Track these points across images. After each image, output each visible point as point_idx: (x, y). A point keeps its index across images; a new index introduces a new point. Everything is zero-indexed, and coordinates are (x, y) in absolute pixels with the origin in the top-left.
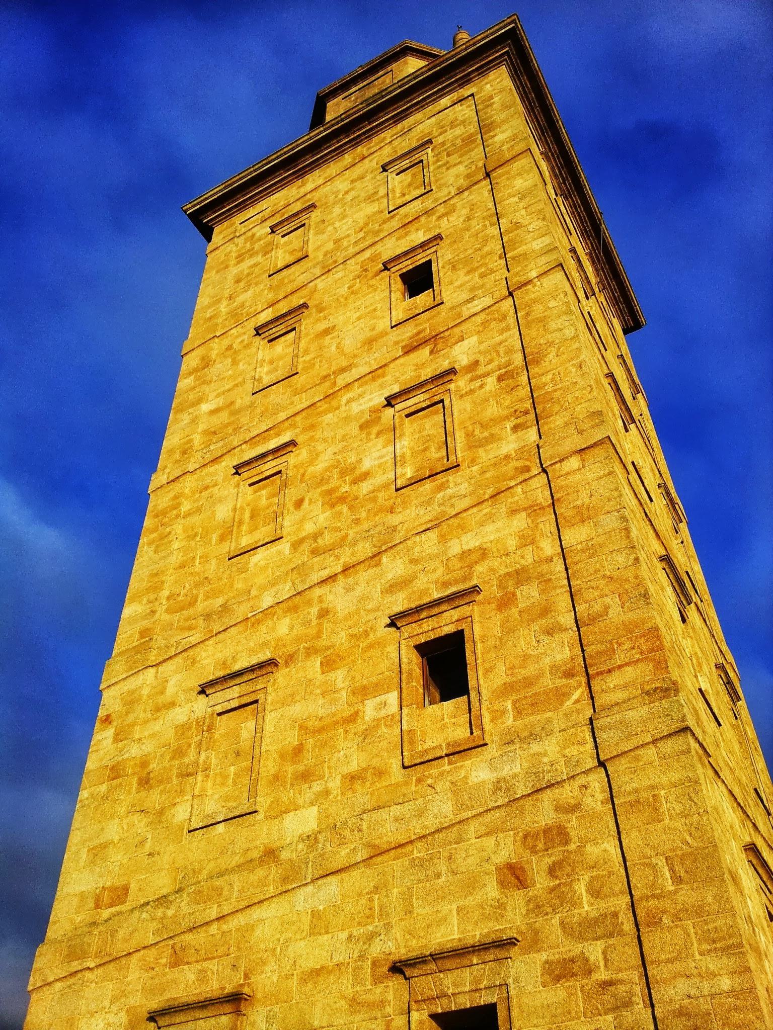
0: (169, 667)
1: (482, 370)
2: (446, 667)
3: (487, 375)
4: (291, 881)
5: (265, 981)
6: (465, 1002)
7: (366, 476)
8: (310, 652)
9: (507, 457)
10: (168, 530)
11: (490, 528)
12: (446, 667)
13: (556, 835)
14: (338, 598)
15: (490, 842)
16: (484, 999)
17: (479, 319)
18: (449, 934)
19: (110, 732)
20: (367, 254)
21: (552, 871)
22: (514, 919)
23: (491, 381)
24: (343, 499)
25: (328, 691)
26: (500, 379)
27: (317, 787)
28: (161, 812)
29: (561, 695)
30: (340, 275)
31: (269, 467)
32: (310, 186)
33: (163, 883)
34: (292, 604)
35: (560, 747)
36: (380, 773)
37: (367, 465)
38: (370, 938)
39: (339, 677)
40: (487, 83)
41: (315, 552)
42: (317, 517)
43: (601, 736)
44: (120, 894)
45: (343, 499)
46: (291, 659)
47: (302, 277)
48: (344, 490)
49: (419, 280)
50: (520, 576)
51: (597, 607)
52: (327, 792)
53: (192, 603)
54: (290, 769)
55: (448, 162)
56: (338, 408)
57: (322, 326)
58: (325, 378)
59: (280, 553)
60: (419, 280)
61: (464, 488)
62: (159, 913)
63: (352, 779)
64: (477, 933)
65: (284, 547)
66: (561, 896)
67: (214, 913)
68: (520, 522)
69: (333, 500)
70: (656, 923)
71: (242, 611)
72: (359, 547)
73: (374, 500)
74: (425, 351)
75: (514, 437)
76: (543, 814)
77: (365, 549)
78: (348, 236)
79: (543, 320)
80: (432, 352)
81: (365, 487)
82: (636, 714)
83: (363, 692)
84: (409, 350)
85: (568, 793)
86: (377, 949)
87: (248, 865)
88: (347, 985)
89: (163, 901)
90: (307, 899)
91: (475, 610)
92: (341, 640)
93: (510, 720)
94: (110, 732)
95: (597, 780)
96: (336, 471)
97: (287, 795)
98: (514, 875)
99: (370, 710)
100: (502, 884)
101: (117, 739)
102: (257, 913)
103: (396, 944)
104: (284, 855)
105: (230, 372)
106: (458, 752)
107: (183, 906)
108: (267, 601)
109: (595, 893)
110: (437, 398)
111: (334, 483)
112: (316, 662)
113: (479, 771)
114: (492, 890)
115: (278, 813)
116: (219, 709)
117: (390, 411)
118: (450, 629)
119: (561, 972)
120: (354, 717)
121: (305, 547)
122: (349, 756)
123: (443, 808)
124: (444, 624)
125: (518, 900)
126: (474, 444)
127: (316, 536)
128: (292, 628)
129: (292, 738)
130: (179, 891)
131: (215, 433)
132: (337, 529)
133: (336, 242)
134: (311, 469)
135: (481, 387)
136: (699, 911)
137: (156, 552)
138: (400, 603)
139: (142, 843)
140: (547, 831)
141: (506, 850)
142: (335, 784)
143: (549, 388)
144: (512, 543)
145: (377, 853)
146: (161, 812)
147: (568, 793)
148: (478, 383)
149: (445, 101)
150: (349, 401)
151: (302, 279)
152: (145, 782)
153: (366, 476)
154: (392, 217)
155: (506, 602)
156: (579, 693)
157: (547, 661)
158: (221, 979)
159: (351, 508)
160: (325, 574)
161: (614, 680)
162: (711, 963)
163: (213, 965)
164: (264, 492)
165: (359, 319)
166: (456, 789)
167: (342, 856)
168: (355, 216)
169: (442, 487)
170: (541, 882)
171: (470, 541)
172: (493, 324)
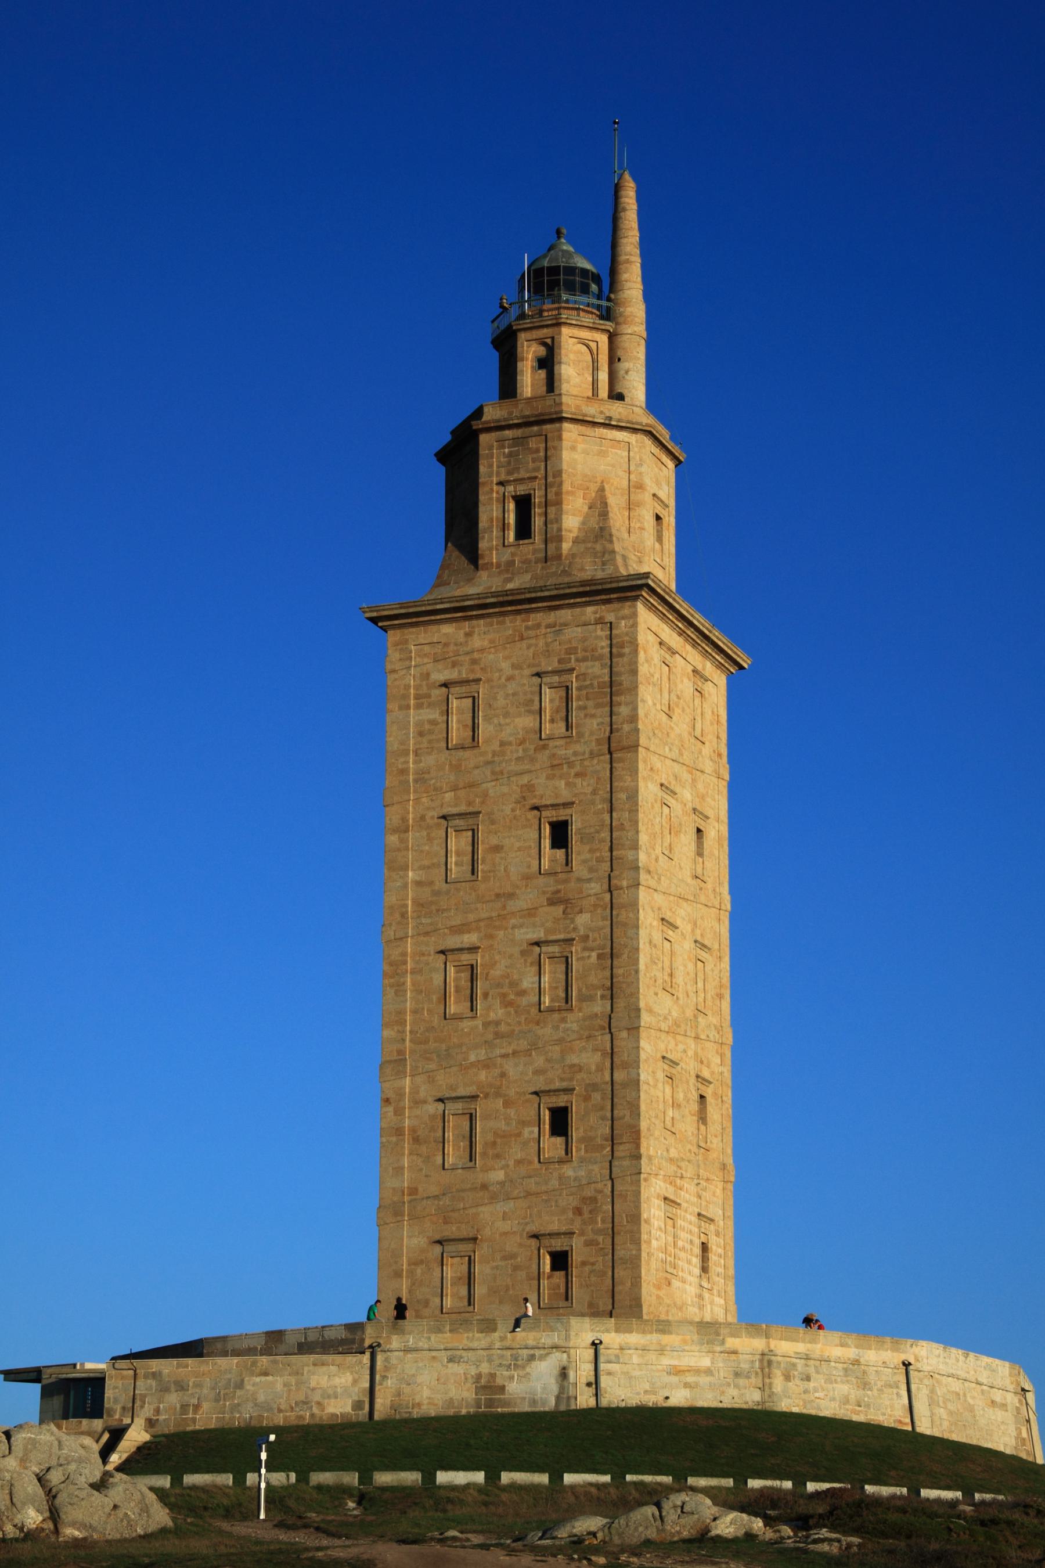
0: (419, 1079)
1: (590, 944)
2: (560, 1121)
3: (592, 950)
4: (494, 1198)
6: (559, 1249)
8: (498, 1095)
9: (596, 1015)
10: (402, 980)
11: (584, 1055)
12: (560, 1121)
13: (593, 1200)
14: (512, 1069)
15: (571, 1198)
17: (592, 899)
18: (554, 1227)
21: (590, 1212)
22: (576, 1227)
23: (594, 954)
24: (511, 1004)
25: (508, 1119)
26: (600, 957)
27: (503, 1162)
28: (428, 1157)
29: (603, 1147)
30: (505, 789)
31: (466, 958)
32: (477, 642)
33: (434, 1190)
34: (487, 1064)
35: (599, 1170)
36: (530, 1163)
38: (527, 1224)
39: (512, 1112)
40: (623, 618)
41: (498, 1035)
42: (498, 1012)
43: (614, 1169)
44: (413, 1191)
45: (511, 1004)
46: (487, 1096)
47: (476, 772)
48: (512, 997)
49: (560, 835)
50: (594, 1087)
51: (621, 1114)
52: (508, 1166)
53: (426, 1042)
54: (491, 1152)
55: (585, 708)
56: (506, 929)
57: (494, 841)
58: (498, 895)
59: (477, 1027)
61: (575, 1026)
62: (436, 1202)
63: (519, 1162)
64: (564, 1229)
65: (479, 1022)
68: (597, 1057)
69: (507, 1004)
70: (619, 1234)
72: (521, 1041)
73: (528, 1012)
74: (561, 908)
75: (599, 1002)
76: (589, 1192)
77: (523, 1044)
78: (510, 743)
79: (625, 925)
80: (564, 912)
81: (524, 1001)
82: (626, 1163)
83: (524, 1123)
84: (551, 902)
85: (600, 1186)
86: (528, 1228)
87: (473, 1189)
88: (518, 1239)
89: (436, 1197)
90: (501, 1207)
92: (512, 1093)
93: (583, 1152)
95: (609, 1183)
96: (507, 981)
98: (578, 1211)
100: (574, 1213)
101: (396, 1113)
102: (481, 1209)
103: (533, 1228)
104: (491, 1188)
105: (427, 848)
106: (561, 1162)
107: (446, 1201)
108: (472, 1058)
109: (603, 1221)
110: (565, 954)
111: (505, 990)
112: (501, 1101)
113: (568, 1171)
114: (570, 1215)
115: (486, 1170)
116: (452, 1112)
117: (537, 949)
118: (562, 1104)
119: (588, 1243)
120: (519, 1135)
121: (491, 1029)
122: (516, 1152)
124: (561, 1101)
125: (578, 1220)
126: (582, 999)
127: (497, 1023)
128: (487, 1077)
129: (490, 1137)
130: (444, 1194)
131: (422, 905)
132: (509, 1024)
133: (502, 744)
134: (492, 972)
135: (589, 957)
136: (632, 1232)
137: (396, 993)
138: (540, 1084)
139: (421, 1170)
140: (590, 1198)
141: (575, 1203)
142: (511, 1163)
143: (621, 979)
144: (593, 1068)
145: (528, 1194)
146: (428, 1157)
148: (586, 954)
150: (513, 928)
152: (416, 1140)
153: (522, 993)
154: (544, 747)
155: (587, 1098)
156: (609, 1149)
157: (599, 1132)
158: (465, 1232)
159: (516, 1012)
160: (503, 1051)
161: (621, 1148)
162: (632, 1247)
163: (463, 1226)
164: (463, 975)
165: (519, 849)
168: (517, 720)
169: (563, 1020)
170: (586, 1215)
171: (573, 1059)
172: (599, 911)
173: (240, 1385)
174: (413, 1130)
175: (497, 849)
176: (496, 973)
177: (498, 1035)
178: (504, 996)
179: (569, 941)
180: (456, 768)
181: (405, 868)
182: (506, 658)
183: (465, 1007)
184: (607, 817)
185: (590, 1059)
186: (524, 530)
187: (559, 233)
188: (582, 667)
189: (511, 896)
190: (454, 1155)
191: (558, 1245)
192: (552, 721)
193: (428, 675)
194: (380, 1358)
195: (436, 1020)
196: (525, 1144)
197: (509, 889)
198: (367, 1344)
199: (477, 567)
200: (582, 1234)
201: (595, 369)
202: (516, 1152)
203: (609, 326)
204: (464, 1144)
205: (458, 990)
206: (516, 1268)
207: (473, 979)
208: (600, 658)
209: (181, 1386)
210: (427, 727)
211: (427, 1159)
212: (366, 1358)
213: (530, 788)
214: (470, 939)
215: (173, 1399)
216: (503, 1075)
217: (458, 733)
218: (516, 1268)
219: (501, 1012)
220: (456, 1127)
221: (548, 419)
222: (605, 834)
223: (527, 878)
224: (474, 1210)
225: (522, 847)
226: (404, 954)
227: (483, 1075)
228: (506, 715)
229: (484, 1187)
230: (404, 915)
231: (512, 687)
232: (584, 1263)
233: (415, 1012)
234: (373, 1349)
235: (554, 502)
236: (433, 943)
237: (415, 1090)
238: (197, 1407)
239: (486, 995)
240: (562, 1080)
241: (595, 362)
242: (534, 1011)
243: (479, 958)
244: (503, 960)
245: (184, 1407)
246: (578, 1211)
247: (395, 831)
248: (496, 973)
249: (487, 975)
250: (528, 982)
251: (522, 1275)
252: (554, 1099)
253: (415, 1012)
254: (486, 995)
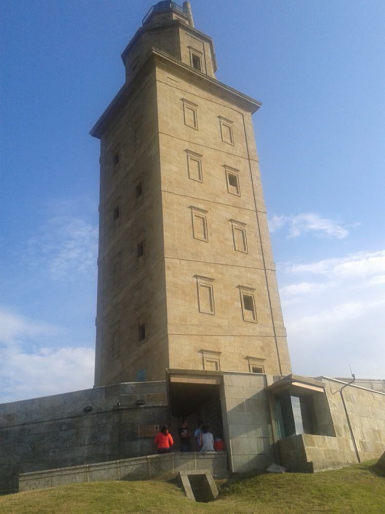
6: (257, 367)
16: (261, 367)
26: (255, 235)
49: (233, 180)
56: (217, 209)
67: (210, 334)
74: (237, 210)
86: (243, 352)
103: (245, 353)
104: (224, 328)
114: (260, 350)
147: (270, 338)
149: (235, 107)
153: (227, 239)
167: (235, 333)
183: (202, 236)
189: (218, 196)
190: (205, 307)
191: (258, 364)
220: (204, 292)
224: (216, 337)
227: (212, 270)
229: (220, 326)
239: (211, 234)
243: (208, 216)
246: (263, 349)
249: (211, 225)
250: (229, 235)
252: (245, 291)
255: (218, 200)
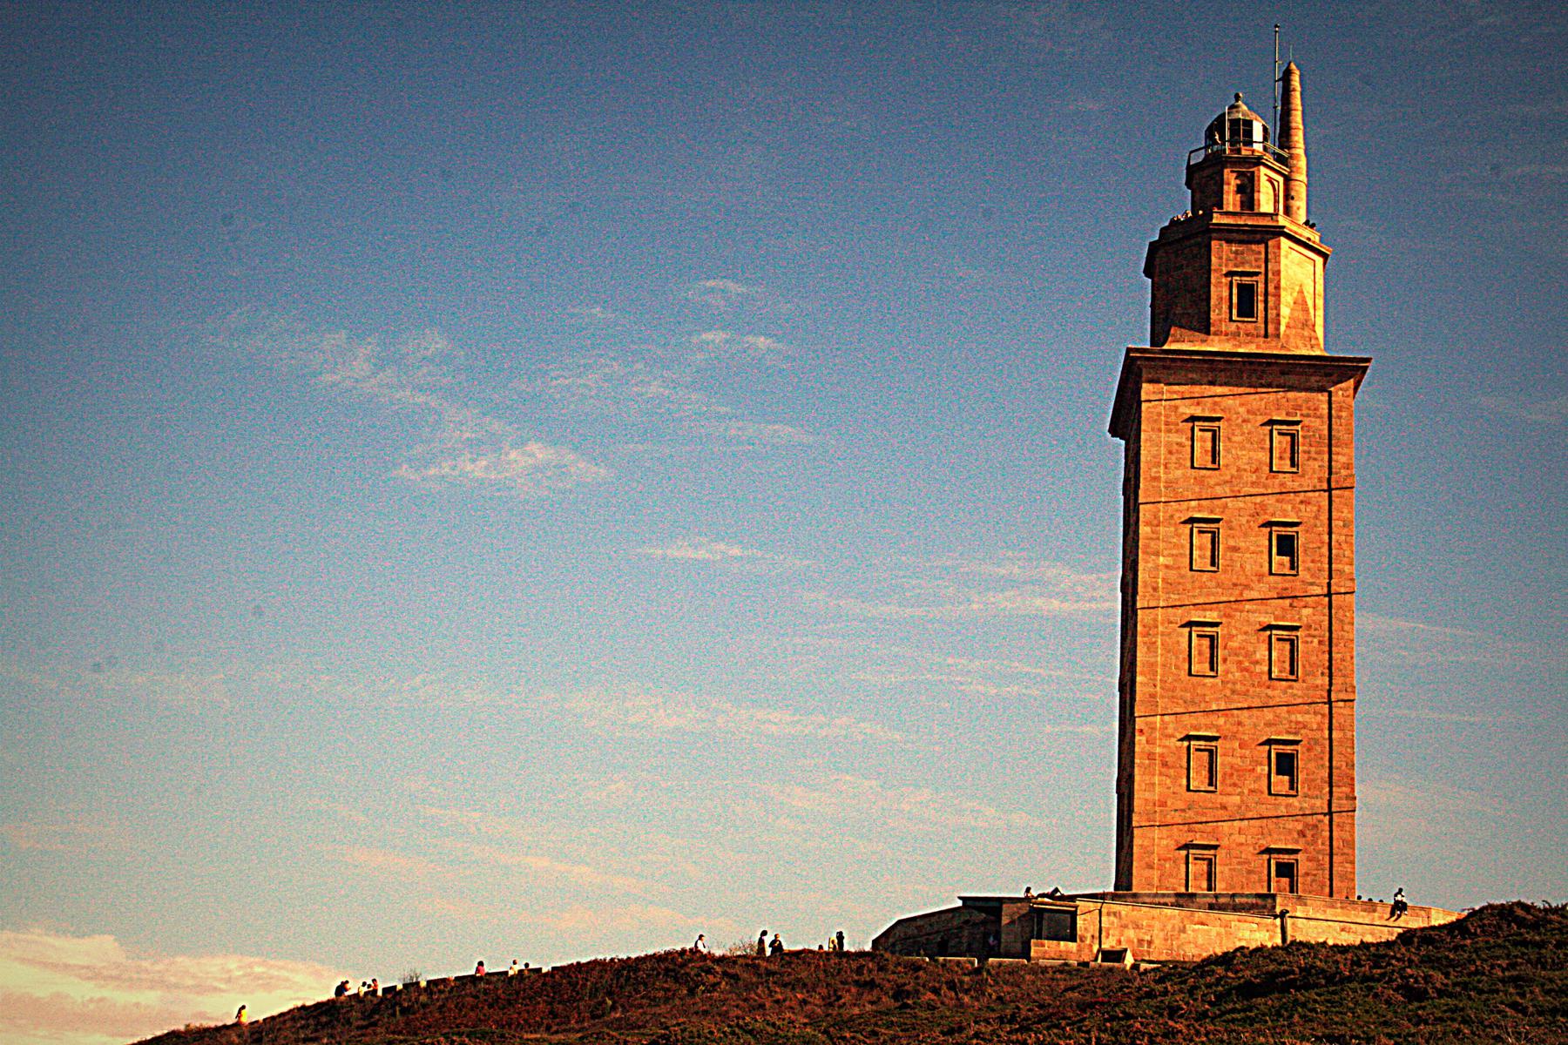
0: (1167, 718)
5: (1224, 842)
7: (1257, 662)
8: (1234, 737)
12: (1286, 765)
19: (1143, 738)
20: (1258, 499)
24: (1246, 670)
26: (1320, 642)
30: (1241, 505)
33: (1181, 805)
37: (1258, 656)
45: (1246, 670)
49: (1287, 546)
50: (1317, 742)
57: (1232, 543)
60: (1287, 546)
63: (1251, 791)
65: (1217, 680)
66: (1314, 842)
71: (1203, 706)
91: (1299, 748)
94: (1143, 738)
97: (1230, 789)
98: (1302, 834)
99: (1259, 769)
103: (1264, 843)
119: (1309, 860)
122: (1250, 784)
123: (1282, 811)
125: (1302, 840)
141: (1300, 827)
151: (1219, 491)
152: (1165, 764)
153: (1257, 662)
166: (1287, 806)
167: (1250, 815)
169: (1291, 687)
173: (1183, 930)
174: (1162, 755)
175: (1235, 549)
176: (1234, 644)
177: (1233, 692)
178: (1240, 662)
179: (1296, 628)
180: (1200, 482)
181: (1157, 554)
182: (1242, 405)
184: (1326, 538)
185: (1313, 719)
186: (1246, 309)
187: (1237, 98)
188: (1306, 421)
189: (1247, 587)
190: (1199, 780)
191: (1285, 858)
192: (1281, 458)
193: (1176, 407)
194: (1289, 922)
195: (1183, 674)
196: (1259, 777)
197: (1243, 580)
198: (1278, 910)
199: (1208, 333)
200: (1306, 851)
201: (1276, 202)
202: (1250, 784)
203: (1286, 171)
204: (1205, 773)
205: (1200, 653)
206: (1249, 872)
207: (1213, 647)
208: (1320, 417)
209: (1137, 927)
210: (1175, 447)
211: (1175, 779)
212: (1278, 921)
213: (1263, 507)
214: (1211, 616)
215: (1131, 933)
216: (1239, 723)
217: (1203, 457)
218: (1249, 872)
219: (1238, 675)
220: (1199, 760)
221: (1268, 234)
222: (1325, 550)
223: (1260, 576)
225: (1250, 551)
226: (1155, 620)
227: (1221, 721)
228: (1243, 448)
229: (1224, 808)
230: (1155, 589)
231: (1247, 427)
232: (1307, 874)
233: (1164, 665)
234: (1283, 915)
235: (1273, 292)
236: (1180, 615)
237: (1165, 725)
238: (1150, 943)
239: (1225, 660)
240: (1289, 733)
241: (1276, 196)
242: (1266, 677)
244: (1239, 634)
245: (1141, 941)
247: (1147, 524)
248: (1234, 644)
250: (1262, 653)
251: (1255, 877)
253: (1164, 665)
254: (1225, 660)
255: (1247, 595)
